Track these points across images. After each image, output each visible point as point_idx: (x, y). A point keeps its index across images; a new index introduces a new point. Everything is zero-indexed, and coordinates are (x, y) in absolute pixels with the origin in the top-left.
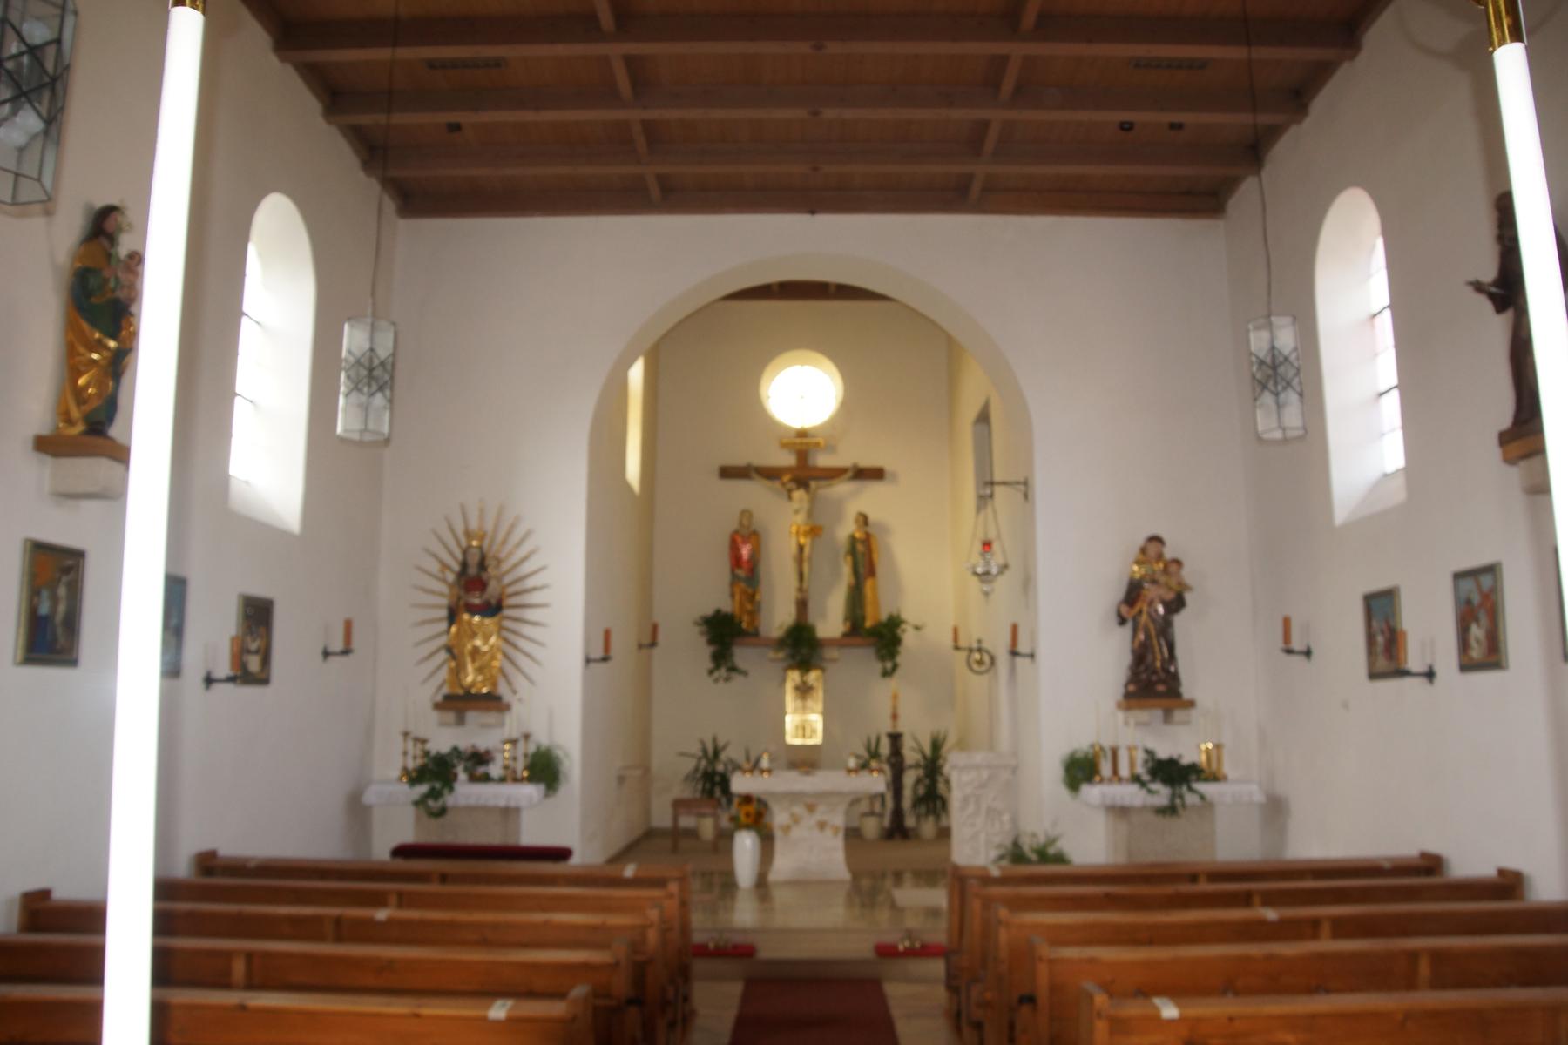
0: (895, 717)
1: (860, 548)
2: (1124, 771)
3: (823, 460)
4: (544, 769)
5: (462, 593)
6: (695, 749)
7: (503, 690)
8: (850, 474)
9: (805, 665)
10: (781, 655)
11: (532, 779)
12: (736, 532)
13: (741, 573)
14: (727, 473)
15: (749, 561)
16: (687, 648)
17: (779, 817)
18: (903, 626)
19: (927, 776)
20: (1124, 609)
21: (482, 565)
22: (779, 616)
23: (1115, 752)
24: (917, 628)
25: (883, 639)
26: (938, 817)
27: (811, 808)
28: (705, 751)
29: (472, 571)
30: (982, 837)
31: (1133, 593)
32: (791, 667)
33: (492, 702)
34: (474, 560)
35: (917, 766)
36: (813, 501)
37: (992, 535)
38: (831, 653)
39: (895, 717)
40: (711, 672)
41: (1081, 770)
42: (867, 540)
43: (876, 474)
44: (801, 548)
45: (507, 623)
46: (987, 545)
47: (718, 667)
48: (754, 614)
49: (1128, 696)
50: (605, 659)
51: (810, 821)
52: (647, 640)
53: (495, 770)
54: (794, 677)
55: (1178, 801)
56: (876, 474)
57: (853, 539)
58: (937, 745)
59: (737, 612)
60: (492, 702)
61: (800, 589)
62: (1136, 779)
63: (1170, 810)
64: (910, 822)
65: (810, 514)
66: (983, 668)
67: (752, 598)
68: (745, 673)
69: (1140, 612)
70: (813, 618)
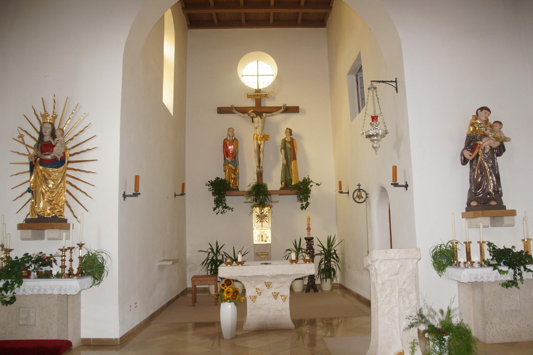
0: (309, 229)
1: (288, 145)
2: (476, 257)
3: (268, 103)
4: (92, 267)
5: (39, 153)
6: (207, 248)
7: (67, 214)
8: (282, 110)
9: (262, 205)
10: (250, 200)
11: (81, 274)
12: (226, 139)
13: (229, 159)
14: (221, 111)
15: (232, 154)
16: (201, 198)
17: (250, 292)
18: (311, 184)
19: (326, 258)
20: (467, 154)
21: (53, 135)
22: (248, 179)
23: (468, 244)
24: (317, 184)
25: (301, 190)
26: (332, 280)
27: (268, 285)
28: (212, 249)
29: (47, 138)
30: (397, 310)
31: (472, 142)
32: (255, 206)
33: (58, 222)
34: (47, 132)
35: (320, 254)
36: (264, 122)
37: (378, 113)
38: (274, 198)
39: (309, 229)
40: (215, 209)
41: (444, 258)
42: (292, 141)
43: (295, 110)
44: (259, 146)
45: (69, 172)
46: (374, 118)
47: (218, 206)
48: (236, 179)
49: (469, 208)
50: (136, 195)
51: (269, 293)
52: (180, 192)
53: (56, 269)
54: (257, 210)
55: (518, 277)
56: (295, 110)
57: (284, 141)
58: (330, 243)
59: (227, 179)
60: (58, 222)
61: (259, 167)
62: (484, 263)
63: (512, 283)
64: (318, 282)
65: (263, 128)
66: (362, 200)
67: (235, 171)
69: (478, 155)
70: (265, 181)
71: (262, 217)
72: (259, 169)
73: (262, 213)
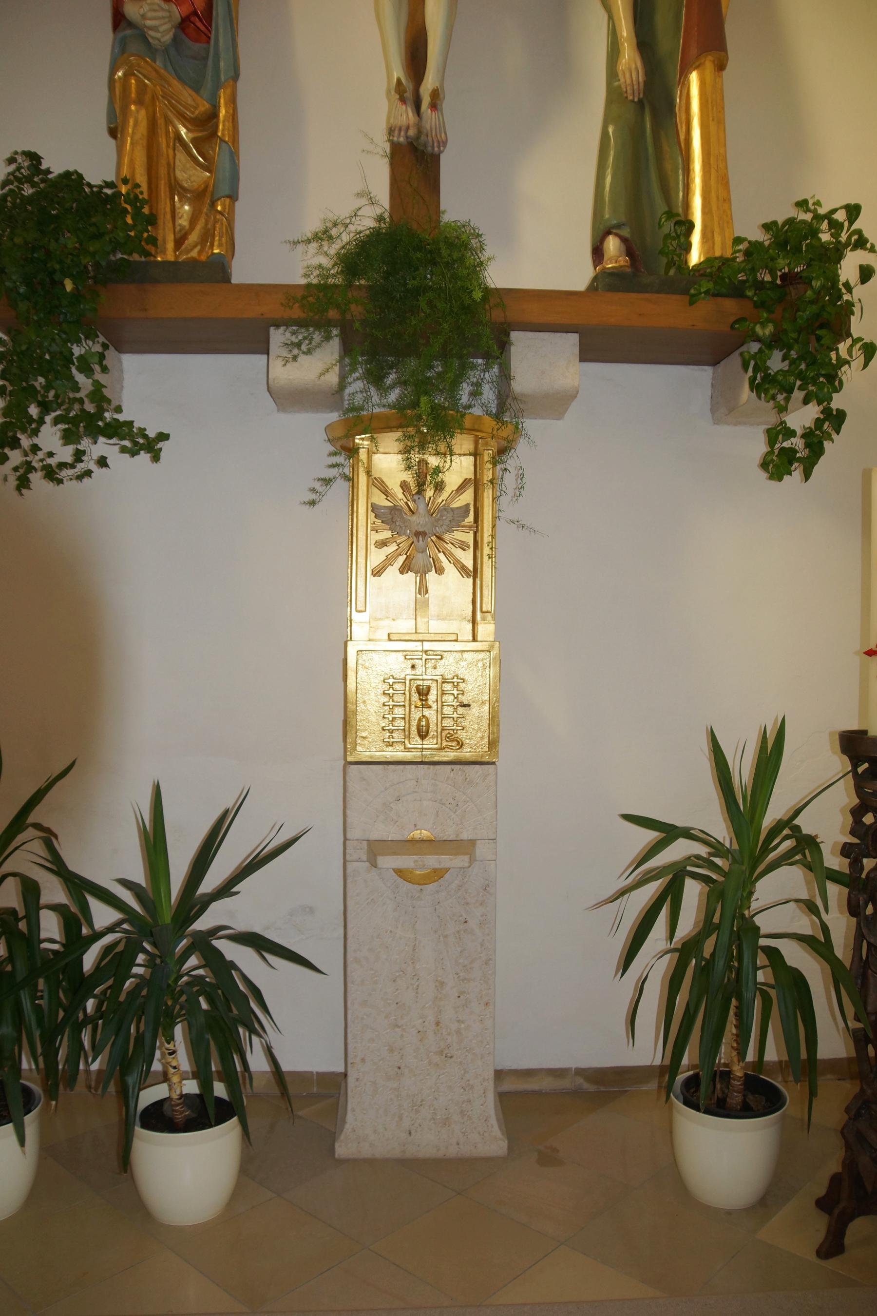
9: (429, 422)
22: (310, 187)
38: (541, 362)
48: (217, 197)
54: (388, 461)
68: (149, 445)
70: (458, 202)
71: (418, 534)
72: (406, 115)
73: (424, 479)
